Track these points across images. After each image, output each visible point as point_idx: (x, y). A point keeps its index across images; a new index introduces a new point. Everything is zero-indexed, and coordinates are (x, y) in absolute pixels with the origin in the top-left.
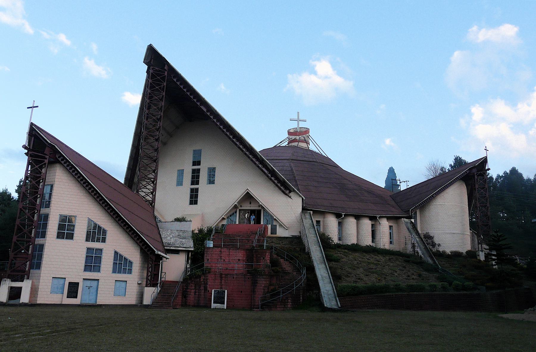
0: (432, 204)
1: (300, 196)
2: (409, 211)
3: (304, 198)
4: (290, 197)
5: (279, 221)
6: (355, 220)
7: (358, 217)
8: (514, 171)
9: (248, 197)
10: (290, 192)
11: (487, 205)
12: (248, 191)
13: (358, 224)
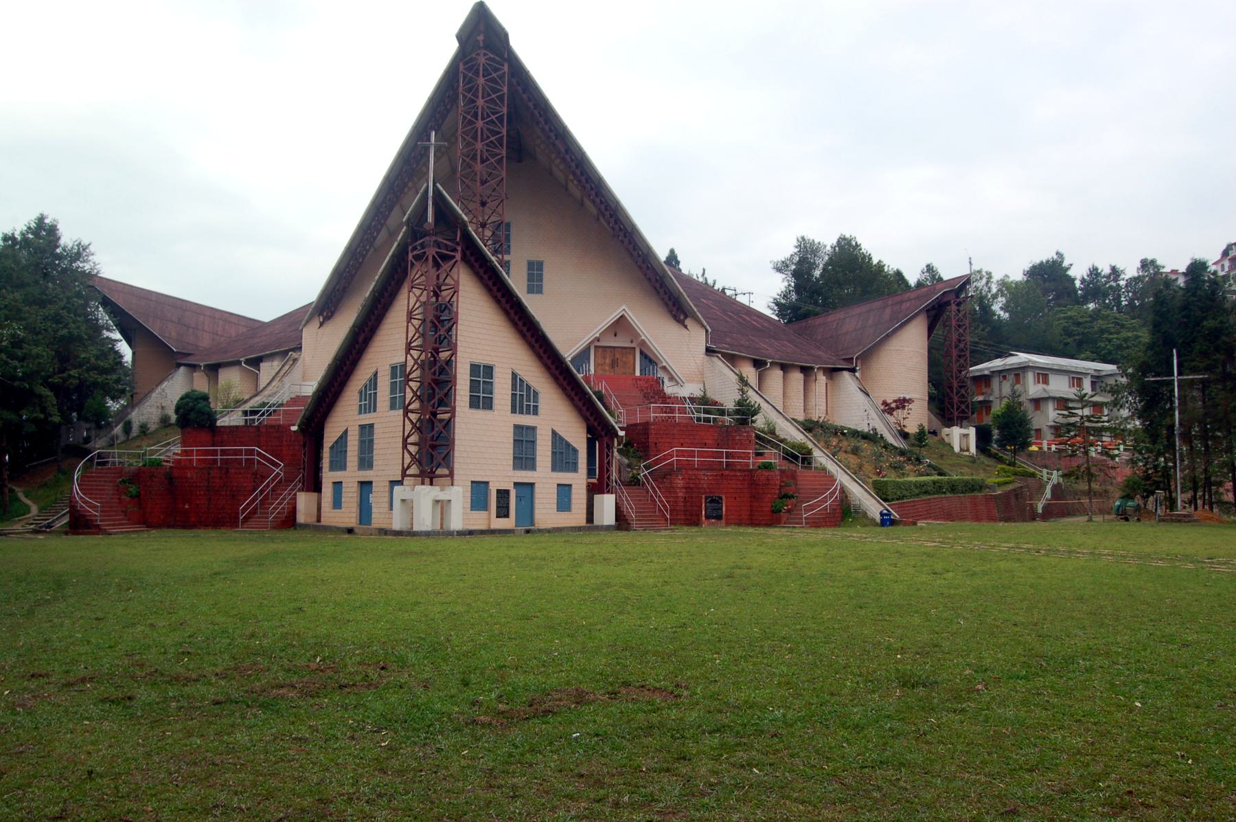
0: (887, 348)
1: (703, 326)
2: (852, 358)
3: (710, 330)
4: (686, 327)
5: (670, 370)
6: (781, 372)
7: (784, 368)
8: (44, 233)
9: (621, 325)
10: (686, 317)
11: (957, 353)
12: (623, 312)
13: (784, 378)
